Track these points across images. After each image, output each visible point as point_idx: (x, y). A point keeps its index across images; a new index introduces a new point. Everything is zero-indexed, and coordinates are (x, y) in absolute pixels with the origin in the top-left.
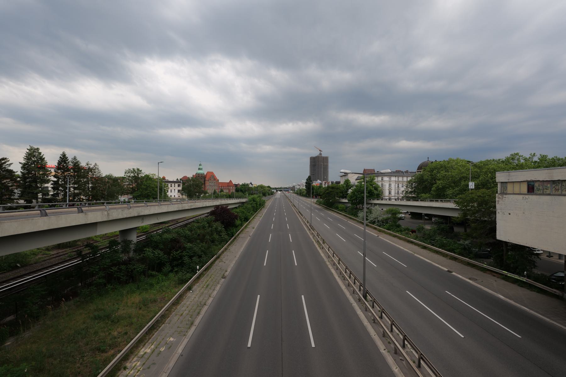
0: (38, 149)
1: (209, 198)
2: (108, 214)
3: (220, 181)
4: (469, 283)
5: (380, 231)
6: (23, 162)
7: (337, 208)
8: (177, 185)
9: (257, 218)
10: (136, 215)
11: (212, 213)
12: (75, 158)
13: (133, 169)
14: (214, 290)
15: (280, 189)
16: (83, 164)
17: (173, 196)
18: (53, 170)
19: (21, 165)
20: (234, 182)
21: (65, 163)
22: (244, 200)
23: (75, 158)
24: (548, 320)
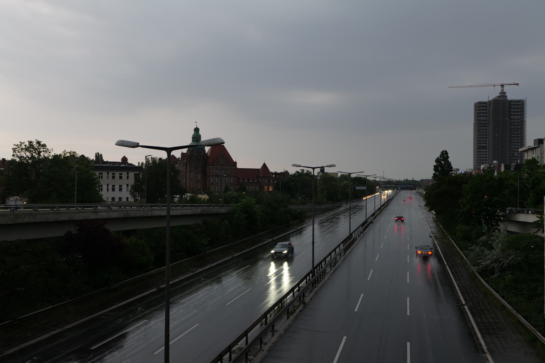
1: (193, 201)
3: (239, 166)
8: (132, 175)
13: (30, 142)
17: (117, 200)
20: (273, 168)
22: (223, 210)
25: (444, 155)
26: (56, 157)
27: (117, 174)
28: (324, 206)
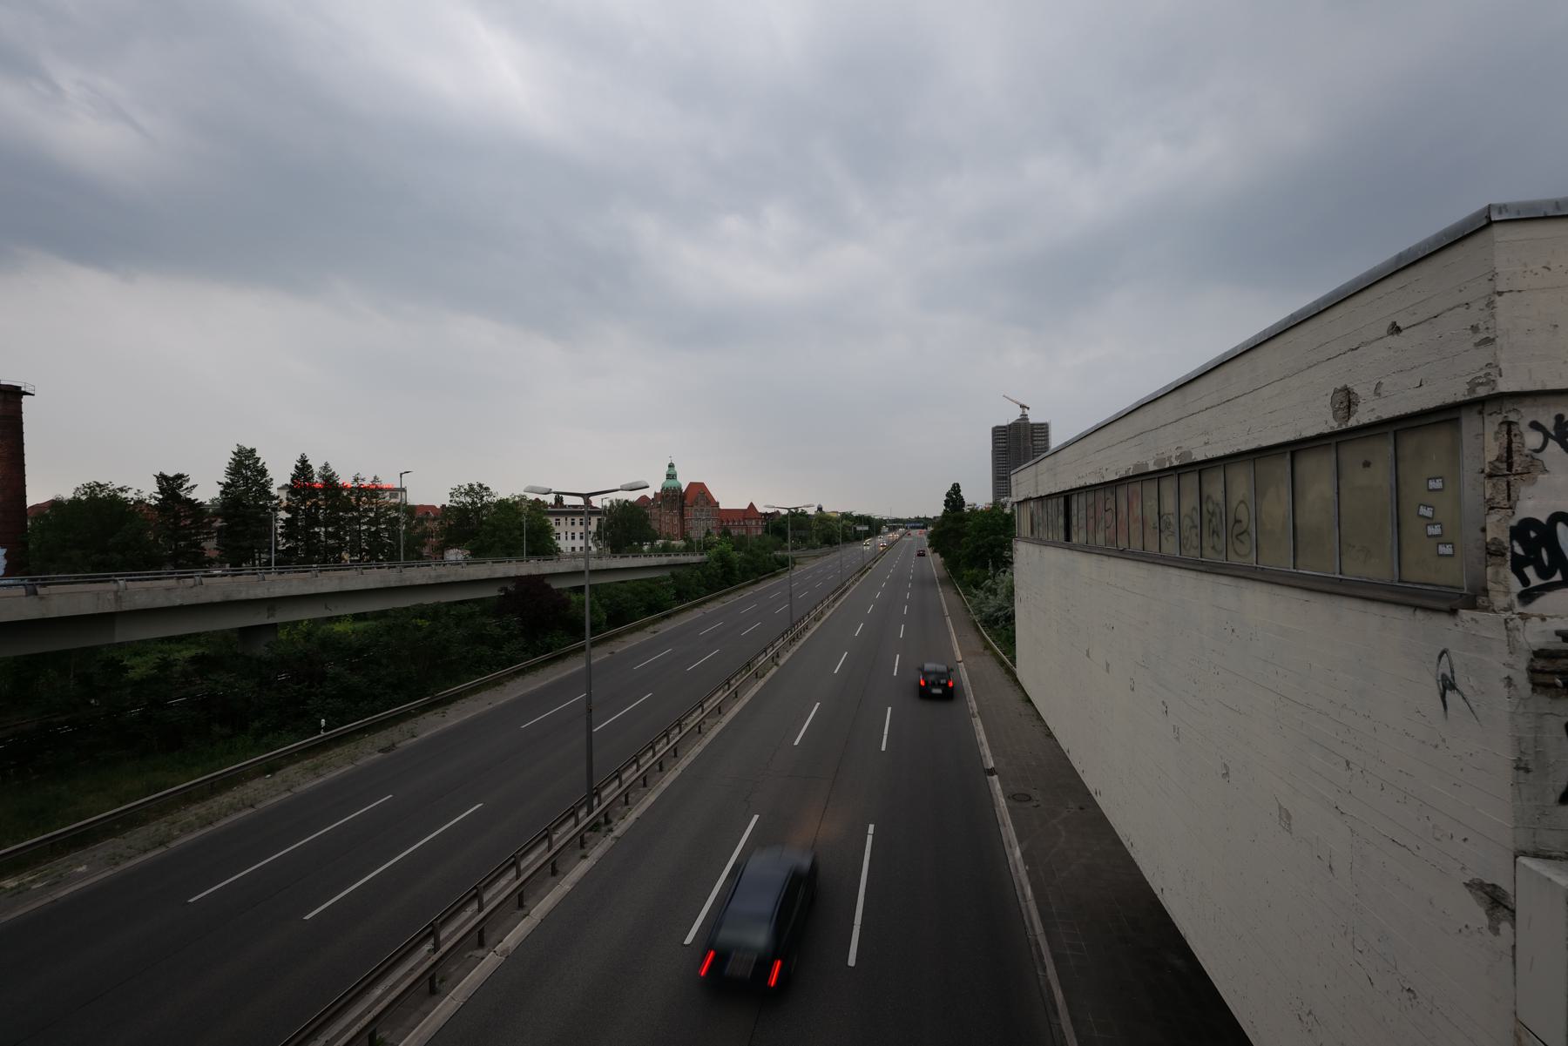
0: (253, 451)
1: (666, 550)
2: (118, 598)
3: (722, 507)
4: (992, 804)
5: (987, 647)
6: (224, 480)
7: (960, 578)
9: (709, 605)
10: (218, 599)
11: (508, 595)
12: (326, 467)
13: (471, 486)
14: (319, 776)
15: (895, 524)
16: (345, 479)
18: (283, 495)
19: (221, 488)
20: (761, 509)
21: (309, 479)
23: (326, 467)
24: (1039, 928)
25: (956, 488)
26: (502, 504)
27: (577, 520)
28: (818, 552)
